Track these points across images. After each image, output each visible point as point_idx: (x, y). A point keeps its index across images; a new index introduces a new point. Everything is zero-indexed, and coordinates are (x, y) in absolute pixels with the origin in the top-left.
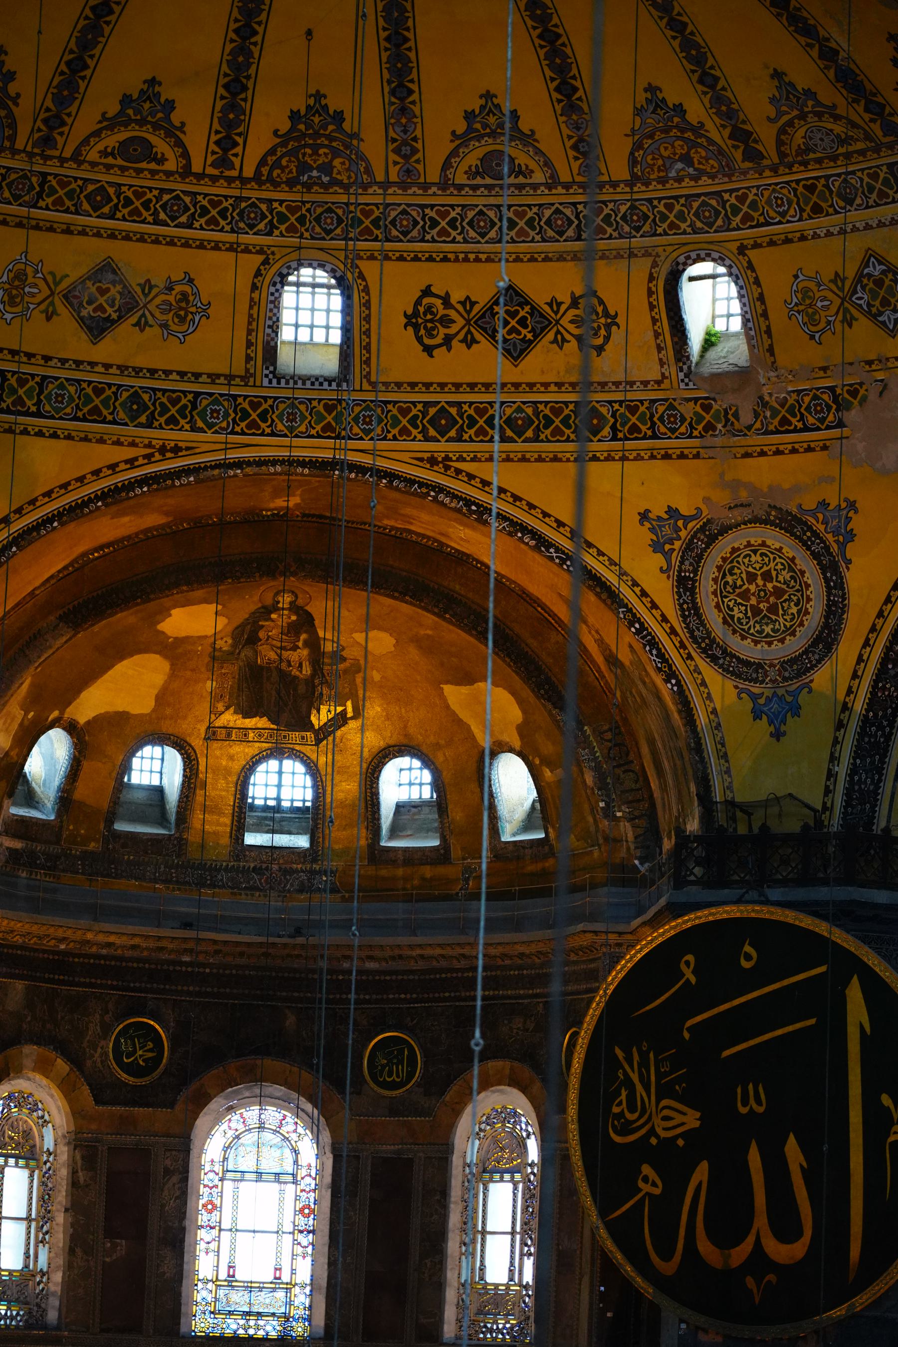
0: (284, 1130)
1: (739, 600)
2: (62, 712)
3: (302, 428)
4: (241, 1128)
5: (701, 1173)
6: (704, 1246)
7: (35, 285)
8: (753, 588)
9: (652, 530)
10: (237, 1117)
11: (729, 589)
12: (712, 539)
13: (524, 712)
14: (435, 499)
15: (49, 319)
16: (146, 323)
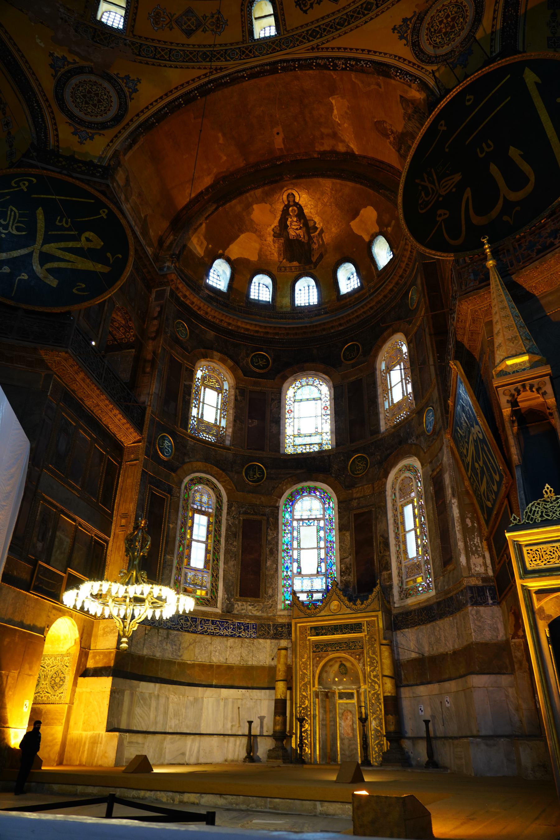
0: (315, 384)
1: (438, 35)
2: (224, 252)
3: (265, 52)
4: (300, 386)
5: (468, 193)
6: (476, 220)
7: (164, 18)
8: (442, 26)
9: (399, 32)
10: (298, 382)
11: (433, 33)
12: (423, 19)
13: (377, 210)
14: (316, 62)
15: (171, 30)
16: (206, 30)
